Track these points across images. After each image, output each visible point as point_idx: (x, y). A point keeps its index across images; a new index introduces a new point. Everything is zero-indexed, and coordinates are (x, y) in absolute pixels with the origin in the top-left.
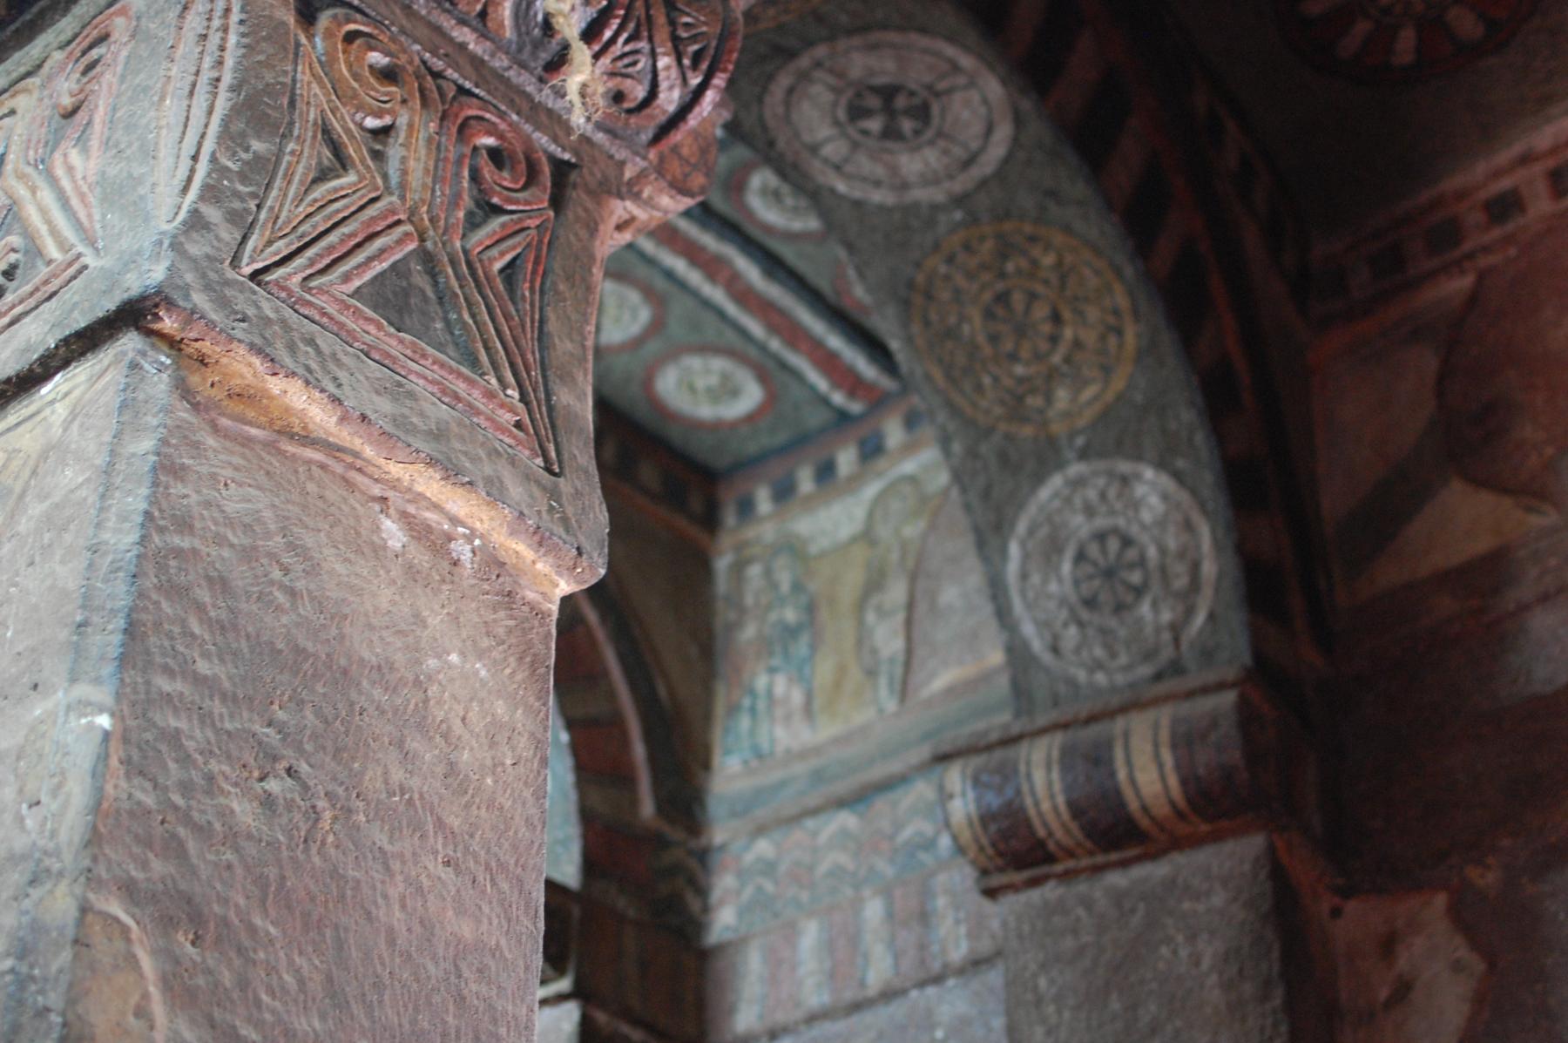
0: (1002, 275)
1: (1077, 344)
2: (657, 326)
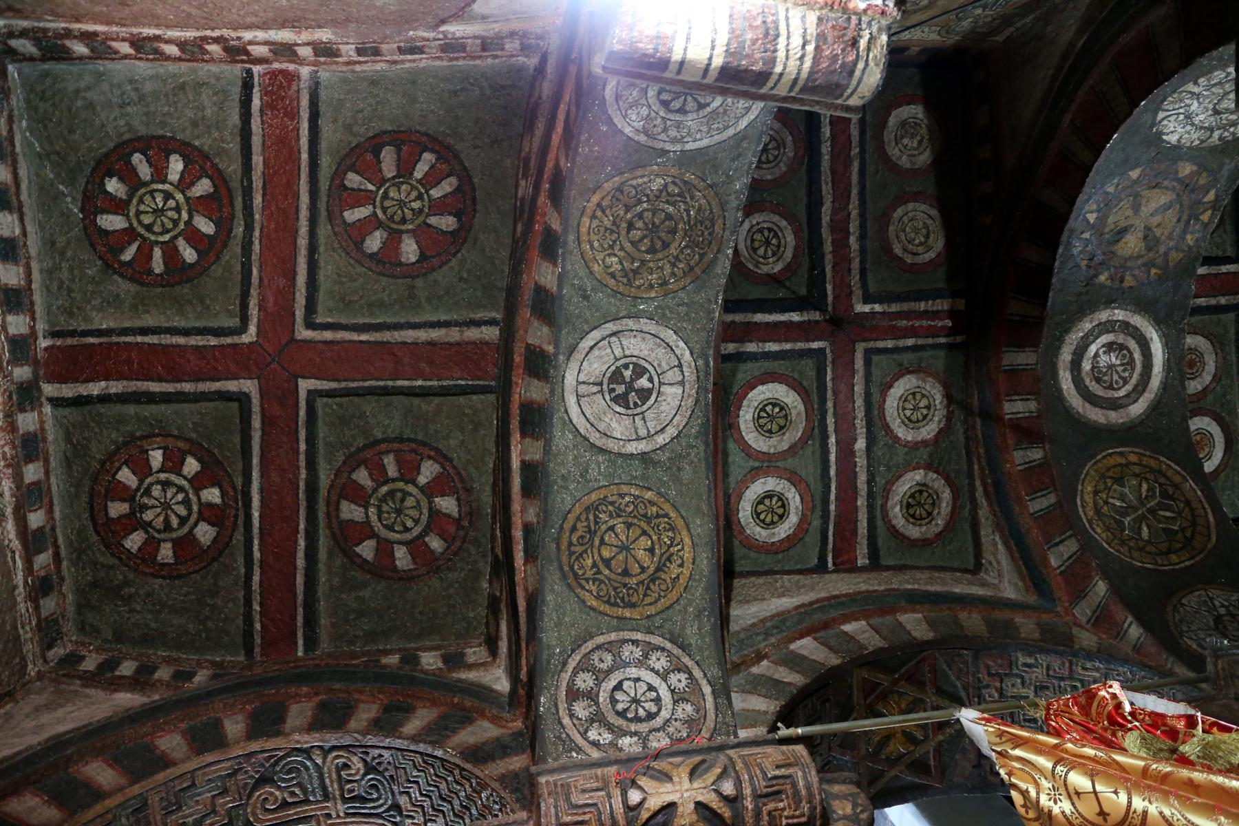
0: (643, 262)
1: (628, 208)
2: (902, 200)
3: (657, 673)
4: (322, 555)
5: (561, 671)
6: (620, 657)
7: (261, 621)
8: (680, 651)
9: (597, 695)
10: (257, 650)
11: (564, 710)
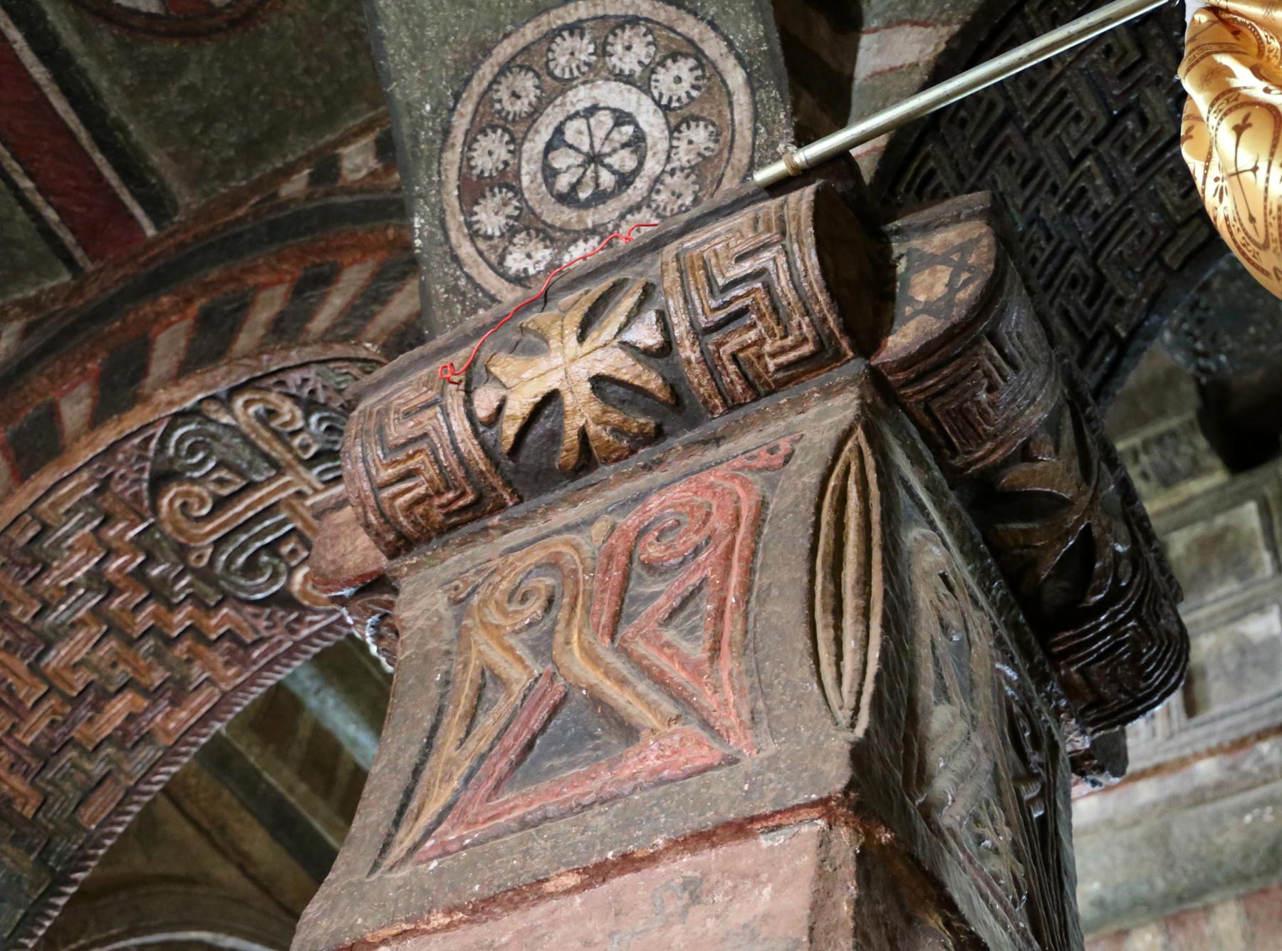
3: (628, 79)
4: (71, 40)
5: (442, 150)
6: (551, 74)
7: (50, 204)
8: (672, 9)
9: (517, 176)
10: (78, 254)
11: (459, 229)
